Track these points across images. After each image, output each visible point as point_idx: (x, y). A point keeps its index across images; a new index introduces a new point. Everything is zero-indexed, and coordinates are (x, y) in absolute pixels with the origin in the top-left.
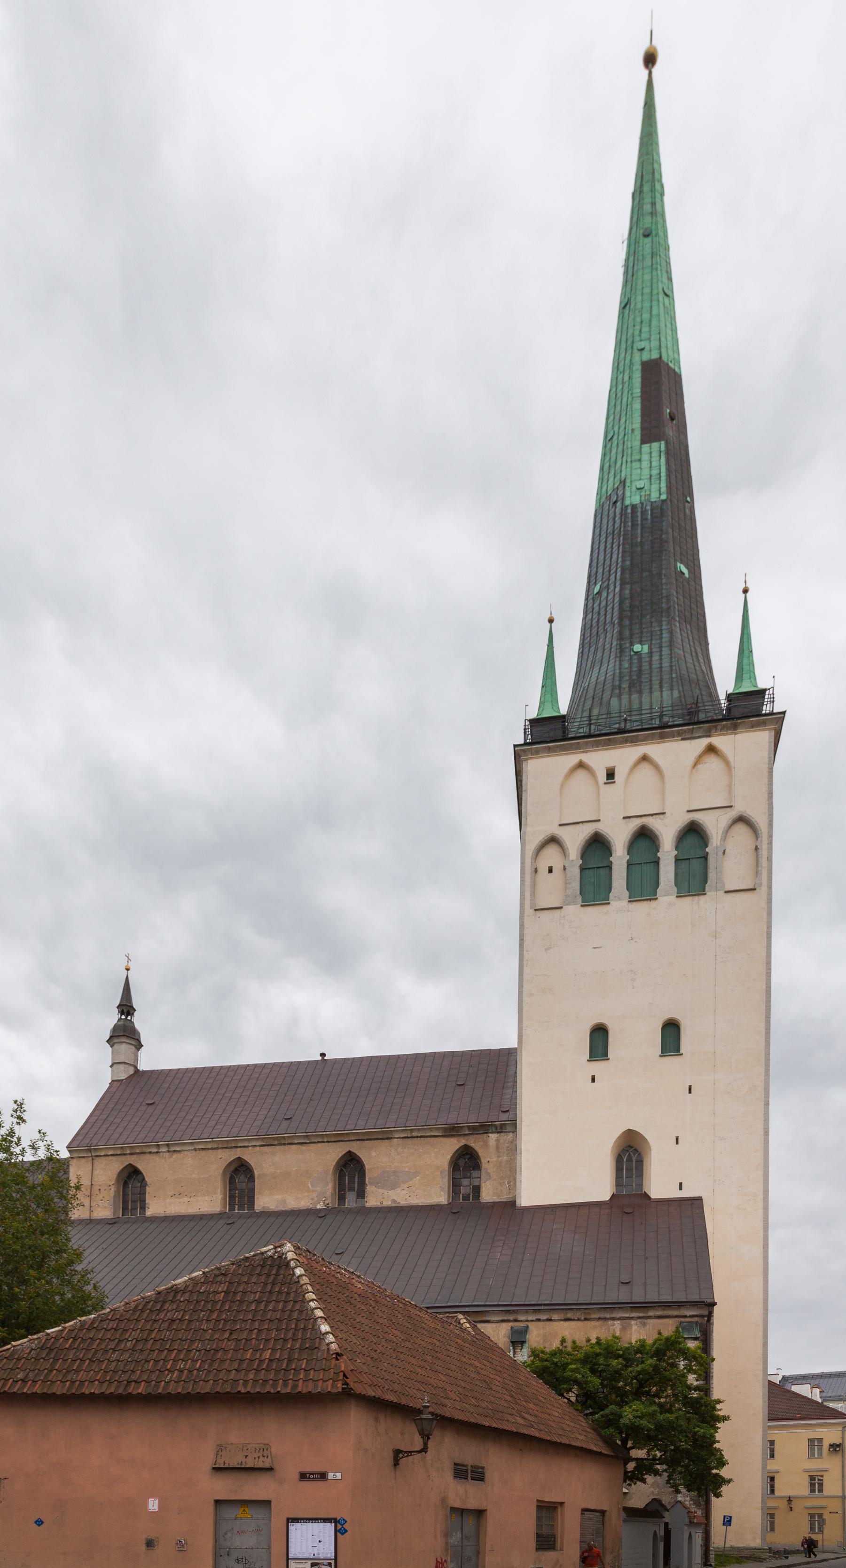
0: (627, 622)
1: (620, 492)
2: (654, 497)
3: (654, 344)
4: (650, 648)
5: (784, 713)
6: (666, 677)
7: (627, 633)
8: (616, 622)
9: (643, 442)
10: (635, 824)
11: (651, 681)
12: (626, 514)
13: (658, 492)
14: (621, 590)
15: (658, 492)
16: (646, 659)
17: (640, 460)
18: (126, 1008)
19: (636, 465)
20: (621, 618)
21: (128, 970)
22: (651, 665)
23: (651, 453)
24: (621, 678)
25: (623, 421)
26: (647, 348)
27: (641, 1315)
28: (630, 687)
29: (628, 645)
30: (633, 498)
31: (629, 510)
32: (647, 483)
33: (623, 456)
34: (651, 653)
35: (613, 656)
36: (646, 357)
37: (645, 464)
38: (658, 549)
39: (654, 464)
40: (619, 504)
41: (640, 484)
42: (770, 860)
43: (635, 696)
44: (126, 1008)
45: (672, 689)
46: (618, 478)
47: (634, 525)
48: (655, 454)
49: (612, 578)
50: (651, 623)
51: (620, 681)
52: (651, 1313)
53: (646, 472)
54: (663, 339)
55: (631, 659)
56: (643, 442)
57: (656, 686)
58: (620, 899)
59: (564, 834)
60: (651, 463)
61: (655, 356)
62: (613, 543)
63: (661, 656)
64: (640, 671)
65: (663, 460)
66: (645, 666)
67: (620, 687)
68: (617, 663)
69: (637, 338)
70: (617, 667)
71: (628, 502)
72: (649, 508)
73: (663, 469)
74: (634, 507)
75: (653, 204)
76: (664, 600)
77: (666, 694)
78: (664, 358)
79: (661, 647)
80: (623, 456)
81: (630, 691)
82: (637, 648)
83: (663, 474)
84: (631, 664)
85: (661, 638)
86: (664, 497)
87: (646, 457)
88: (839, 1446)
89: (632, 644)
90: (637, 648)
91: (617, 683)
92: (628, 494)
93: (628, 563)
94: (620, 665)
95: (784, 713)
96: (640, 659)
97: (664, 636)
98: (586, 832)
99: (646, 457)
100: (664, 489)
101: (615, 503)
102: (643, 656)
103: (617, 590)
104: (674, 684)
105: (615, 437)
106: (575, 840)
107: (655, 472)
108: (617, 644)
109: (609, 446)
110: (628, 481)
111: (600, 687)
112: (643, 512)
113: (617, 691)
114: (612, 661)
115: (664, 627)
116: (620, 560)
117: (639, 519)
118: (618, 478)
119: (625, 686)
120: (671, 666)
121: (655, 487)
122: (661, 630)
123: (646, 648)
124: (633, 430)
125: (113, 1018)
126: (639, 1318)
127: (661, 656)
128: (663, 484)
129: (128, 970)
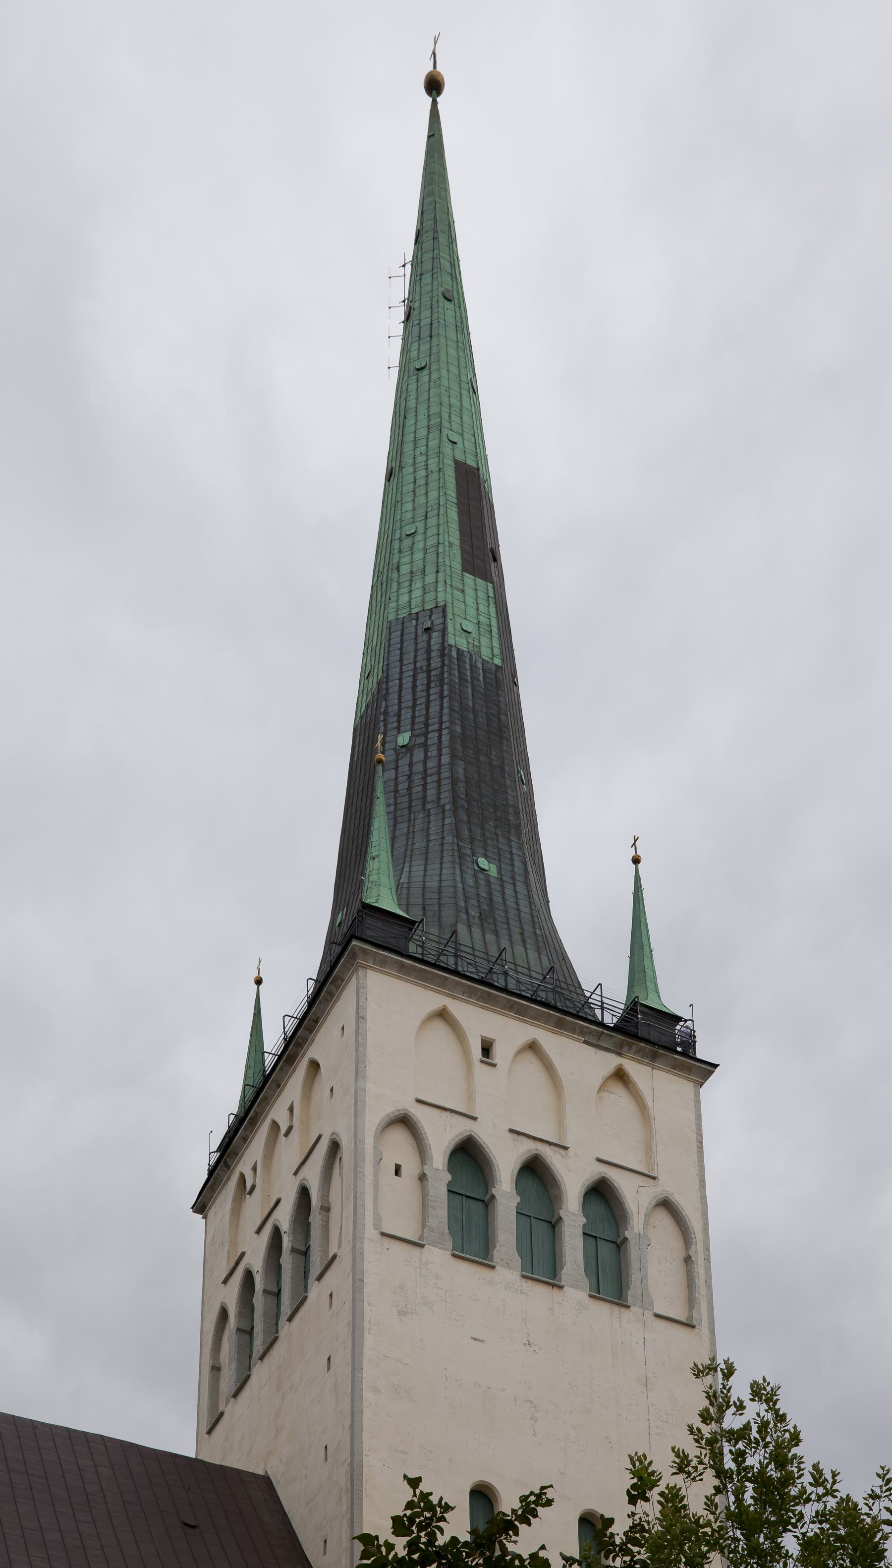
1: (437, 619)
7: (465, 833)
8: (448, 807)
9: (464, 569)
11: (508, 924)
16: (496, 887)
29: (469, 852)
31: (454, 654)
33: (438, 572)
39: (481, 607)
46: (430, 597)
49: (433, 738)
60: (478, 603)
62: (428, 688)
68: (458, 872)
72: (479, 665)
73: (494, 622)
80: (438, 572)
82: (483, 862)
83: (495, 630)
87: (469, 592)
90: (483, 862)
93: (458, 729)
100: (497, 651)
102: (492, 880)
103: (445, 759)
104: (541, 945)
108: (453, 842)
110: (449, 611)
112: (473, 667)
117: (469, 673)
118: (430, 597)
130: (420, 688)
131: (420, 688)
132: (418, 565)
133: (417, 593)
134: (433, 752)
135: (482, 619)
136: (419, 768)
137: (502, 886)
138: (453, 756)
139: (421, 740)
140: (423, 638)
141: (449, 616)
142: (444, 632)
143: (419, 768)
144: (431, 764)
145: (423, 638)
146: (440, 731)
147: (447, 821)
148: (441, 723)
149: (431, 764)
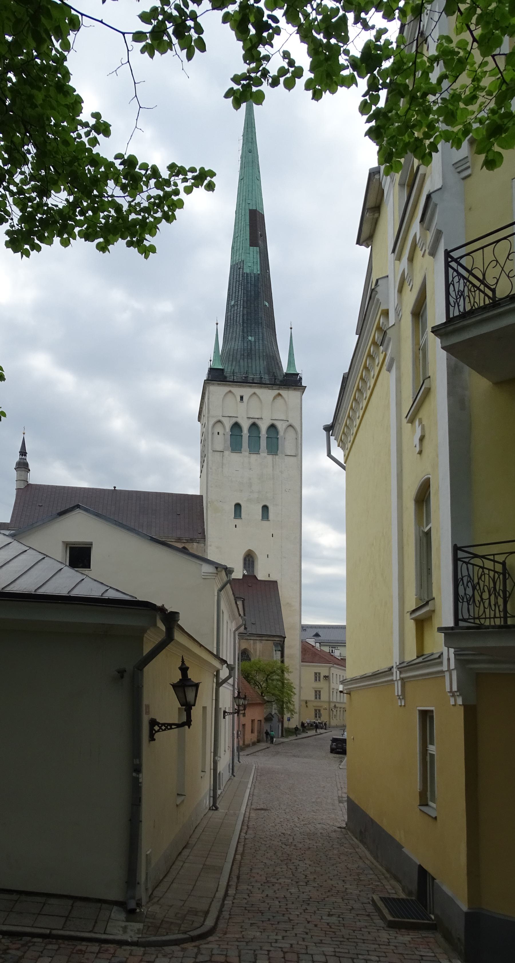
0: (245, 325)
2: (255, 272)
3: (254, 202)
4: (255, 339)
5: (306, 387)
6: (261, 354)
9: (250, 246)
10: (251, 421)
12: (244, 276)
13: (257, 270)
14: (243, 310)
15: (257, 270)
16: (253, 344)
17: (249, 253)
18: (23, 453)
19: (248, 255)
20: (243, 322)
21: (24, 434)
22: (255, 347)
23: (253, 251)
24: (244, 350)
25: (242, 232)
26: (251, 203)
27: (260, 639)
28: (247, 356)
30: (247, 270)
31: (245, 275)
32: (252, 265)
34: (255, 341)
35: (240, 339)
36: (251, 208)
37: (251, 255)
38: (257, 295)
39: (255, 257)
40: (241, 270)
41: (250, 264)
42: (301, 444)
43: (250, 361)
44: (23, 453)
45: (264, 361)
47: (247, 283)
48: (255, 252)
50: (255, 327)
51: (244, 352)
52: (264, 638)
53: (252, 259)
54: (257, 201)
55: (247, 343)
56: (250, 246)
57: (257, 358)
58: (245, 451)
59: (223, 419)
61: (254, 208)
63: (259, 344)
64: (251, 349)
65: (258, 256)
66: (253, 347)
67: (244, 355)
69: (247, 198)
70: (242, 345)
71: (245, 271)
73: (259, 260)
74: (247, 274)
75: (252, 139)
76: (260, 319)
77: (261, 362)
78: (258, 210)
79: (259, 339)
81: (248, 358)
82: (250, 338)
83: (259, 262)
84: (248, 345)
85: (259, 336)
86: (259, 272)
87: (251, 253)
88: (327, 677)
89: (248, 336)
90: (250, 338)
91: (242, 353)
92: (245, 268)
94: (243, 344)
95: (306, 387)
96: (251, 343)
97: (260, 335)
98: (233, 421)
99: (251, 253)
100: (259, 269)
101: (240, 268)
103: (242, 309)
105: (239, 238)
106: (228, 424)
107: (255, 260)
109: (236, 239)
111: (235, 351)
113: (242, 357)
114: (240, 341)
115: (260, 331)
116: (242, 296)
118: (240, 258)
119: (245, 355)
120: (263, 350)
121: (255, 267)
122: (259, 332)
123: (253, 340)
124: (246, 239)
125: (17, 458)
126: (259, 640)
127: (259, 344)
128: (259, 267)
129: (24, 434)
130: (237, 287)
131: (237, 287)
132: (238, 247)
133: (238, 256)
134: (239, 307)
135: (255, 260)
136: (236, 311)
137: (255, 343)
138: (243, 308)
139: (236, 303)
140: (238, 271)
141: (245, 263)
142: (243, 269)
143: (236, 311)
144: (238, 310)
145: (238, 271)
146: (241, 300)
147: (241, 328)
148: (241, 297)
149: (238, 310)
